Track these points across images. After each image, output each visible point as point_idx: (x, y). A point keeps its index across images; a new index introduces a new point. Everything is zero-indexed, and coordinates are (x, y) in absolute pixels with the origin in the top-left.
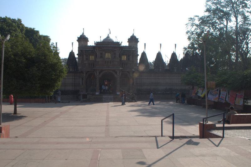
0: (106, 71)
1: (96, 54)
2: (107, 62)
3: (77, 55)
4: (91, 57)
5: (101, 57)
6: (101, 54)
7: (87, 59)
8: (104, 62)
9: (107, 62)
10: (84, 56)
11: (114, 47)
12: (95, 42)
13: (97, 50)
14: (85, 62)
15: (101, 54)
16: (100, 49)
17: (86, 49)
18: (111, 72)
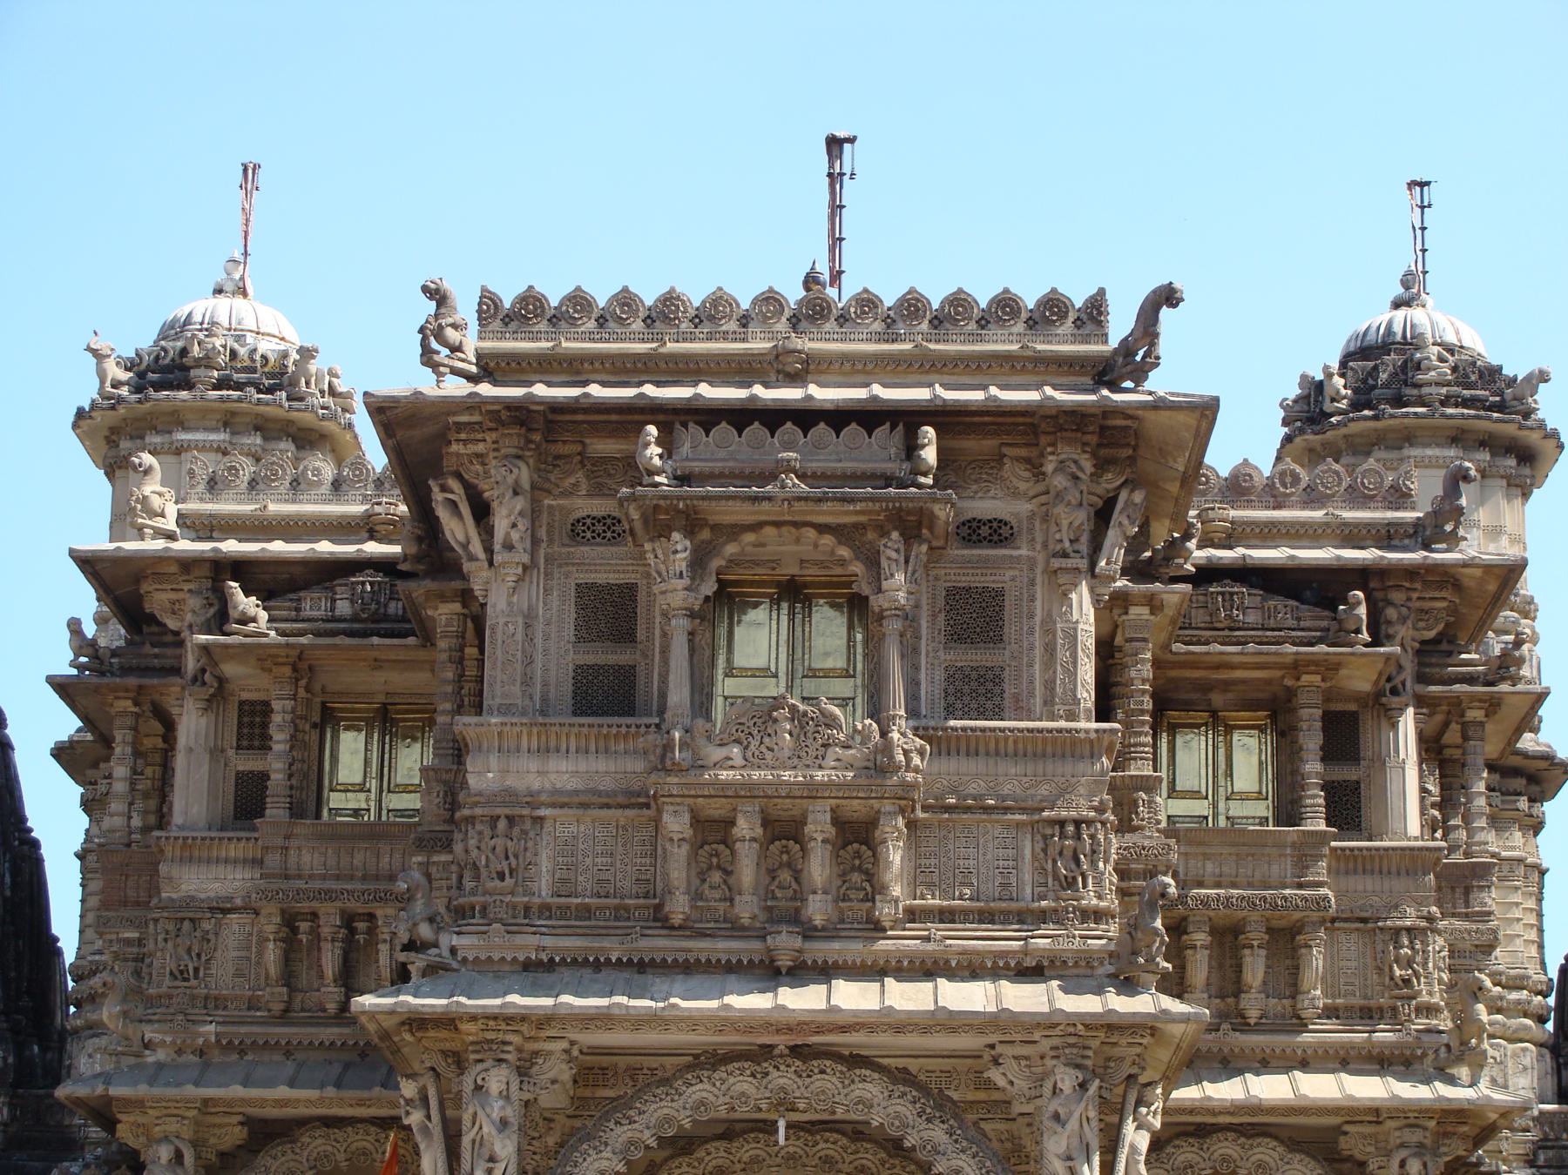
0: (738, 1090)
1: (477, 620)
2: (746, 827)
3: (64, 754)
4: (351, 753)
5: (609, 696)
6: (612, 613)
7: (248, 802)
8: (676, 824)
9: (746, 827)
10: (192, 724)
11: (946, 418)
12: (437, 295)
13: (482, 512)
14: (194, 882)
15: (612, 613)
16: (588, 506)
17: (231, 546)
18: (880, 1104)
